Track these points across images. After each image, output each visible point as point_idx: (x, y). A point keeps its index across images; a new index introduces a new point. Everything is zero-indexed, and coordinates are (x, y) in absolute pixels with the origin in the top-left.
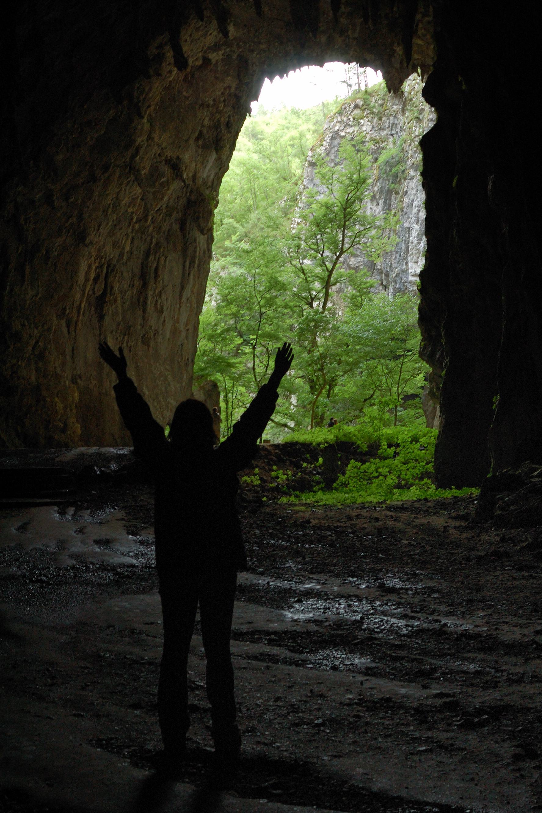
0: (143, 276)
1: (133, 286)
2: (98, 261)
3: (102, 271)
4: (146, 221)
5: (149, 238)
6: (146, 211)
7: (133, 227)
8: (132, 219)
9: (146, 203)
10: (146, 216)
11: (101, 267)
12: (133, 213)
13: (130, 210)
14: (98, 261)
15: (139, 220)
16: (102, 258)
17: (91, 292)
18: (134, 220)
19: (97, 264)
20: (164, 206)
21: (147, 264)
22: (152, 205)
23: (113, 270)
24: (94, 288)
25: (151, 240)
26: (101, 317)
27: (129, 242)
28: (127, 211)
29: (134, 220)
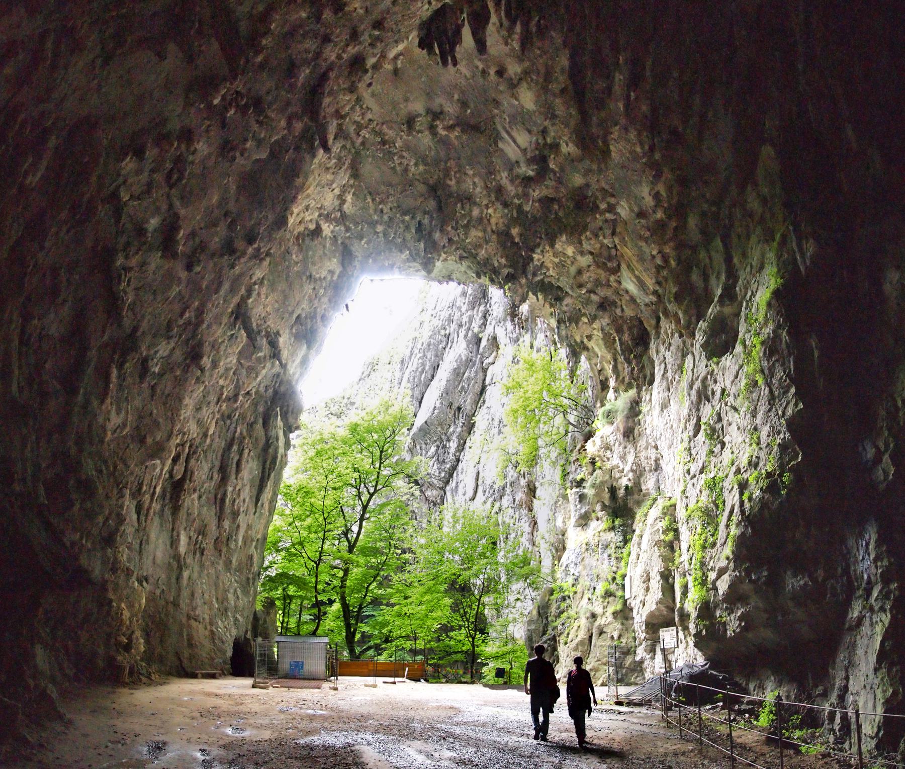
0: (223, 470)
1: (212, 478)
2: (180, 437)
3: (183, 450)
4: (236, 401)
5: (234, 425)
6: (238, 388)
7: (221, 406)
8: (222, 394)
9: (238, 379)
10: (236, 396)
11: (183, 445)
12: (223, 387)
13: (221, 382)
14: (180, 437)
15: (228, 399)
16: (184, 434)
17: (167, 476)
18: (224, 396)
19: (178, 441)
20: (254, 390)
21: (229, 455)
22: (244, 383)
23: (195, 453)
24: (173, 469)
25: (236, 428)
26: (176, 509)
27: (214, 424)
28: (218, 382)
29: (224, 396)
